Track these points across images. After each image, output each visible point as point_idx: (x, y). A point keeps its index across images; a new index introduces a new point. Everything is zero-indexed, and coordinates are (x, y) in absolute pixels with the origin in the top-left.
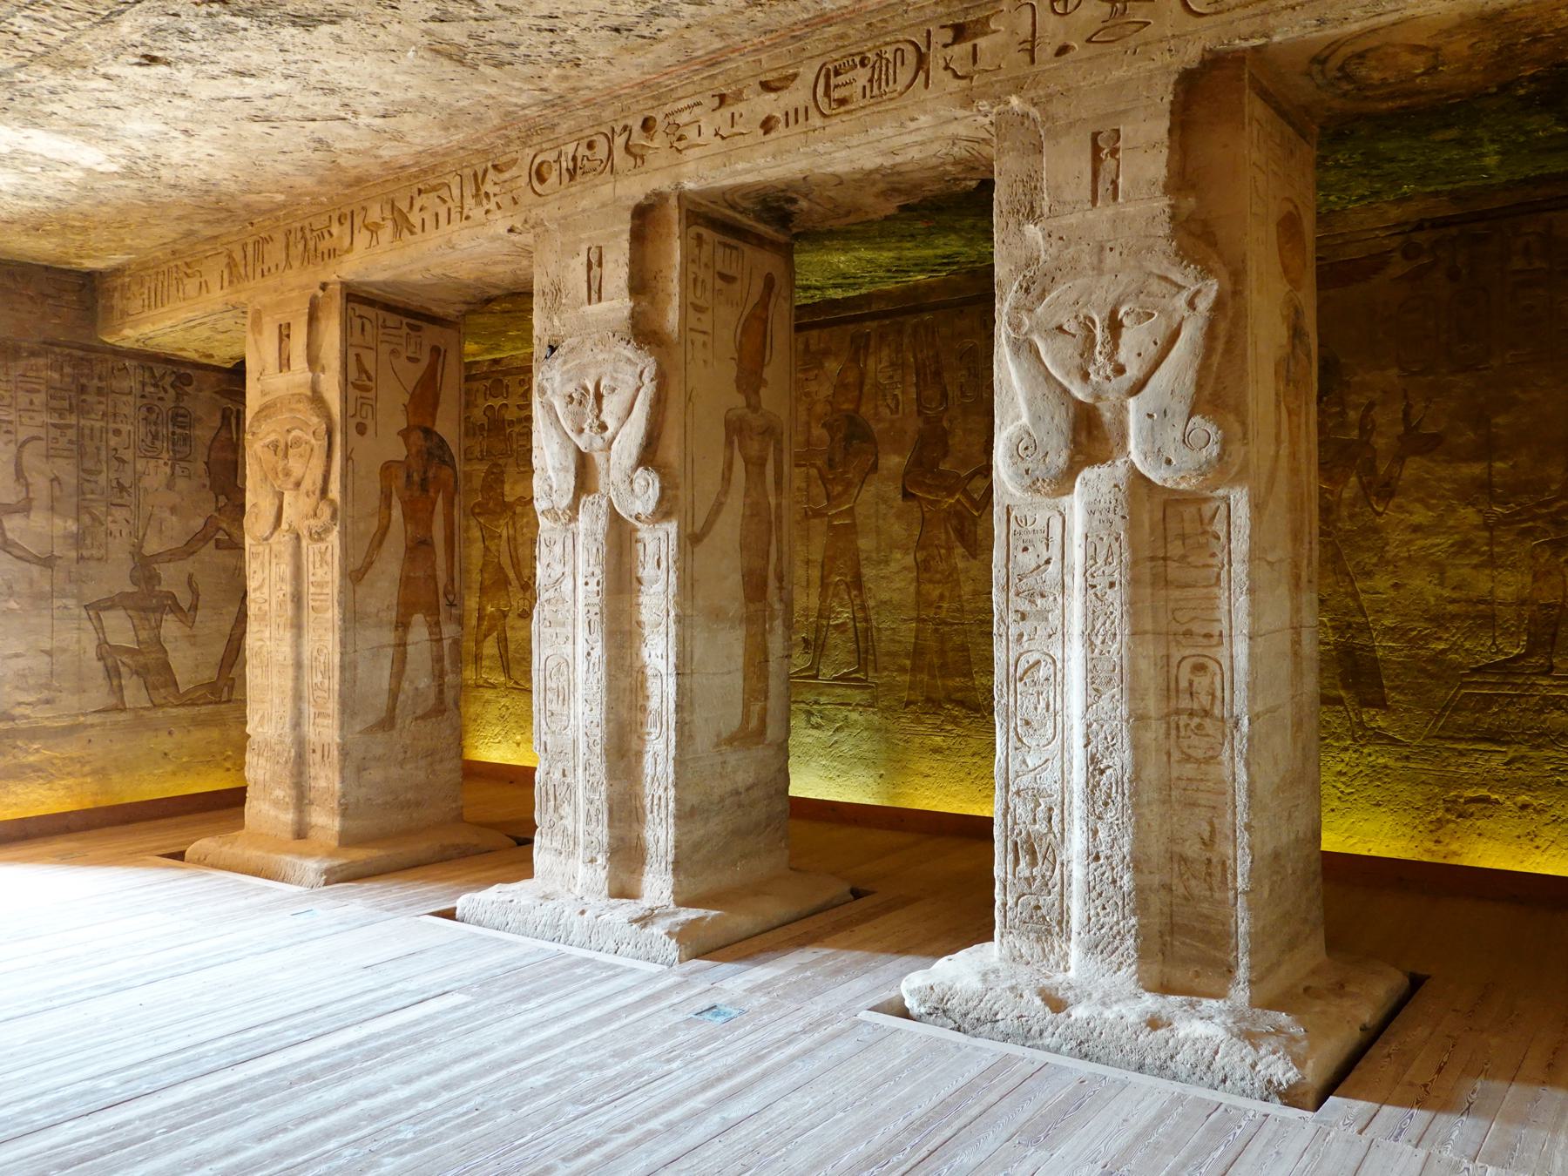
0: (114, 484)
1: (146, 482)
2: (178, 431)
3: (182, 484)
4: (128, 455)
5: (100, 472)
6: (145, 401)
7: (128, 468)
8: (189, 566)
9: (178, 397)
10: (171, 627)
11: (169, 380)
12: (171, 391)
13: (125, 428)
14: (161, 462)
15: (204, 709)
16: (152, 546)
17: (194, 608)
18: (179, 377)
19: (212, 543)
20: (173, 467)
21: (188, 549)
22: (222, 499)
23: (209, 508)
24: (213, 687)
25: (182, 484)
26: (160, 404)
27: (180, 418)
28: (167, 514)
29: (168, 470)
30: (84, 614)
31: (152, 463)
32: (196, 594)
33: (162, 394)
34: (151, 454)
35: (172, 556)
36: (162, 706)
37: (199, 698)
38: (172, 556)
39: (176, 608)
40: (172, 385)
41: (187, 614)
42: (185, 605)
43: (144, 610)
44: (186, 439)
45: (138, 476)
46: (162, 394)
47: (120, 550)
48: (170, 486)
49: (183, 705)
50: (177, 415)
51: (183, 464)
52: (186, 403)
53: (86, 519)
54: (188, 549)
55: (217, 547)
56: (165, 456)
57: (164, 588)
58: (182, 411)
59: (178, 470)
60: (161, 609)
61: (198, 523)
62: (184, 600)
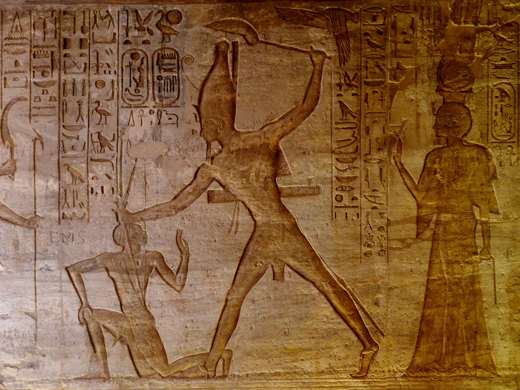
0: (95, 138)
2: (164, 74)
3: (168, 132)
5: (82, 127)
6: (128, 47)
7: (111, 120)
8: (176, 222)
9: (165, 37)
11: (154, 20)
12: (158, 33)
13: (109, 78)
14: (146, 111)
18: (166, 15)
19: (204, 197)
20: (159, 115)
22: (215, 146)
23: (199, 157)
24: (204, 359)
26: (143, 47)
27: (168, 62)
28: (152, 167)
29: (154, 118)
30: (65, 276)
31: (137, 112)
33: (147, 37)
34: (134, 103)
35: (158, 212)
36: (148, 377)
37: (190, 370)
38: (158, 212)
39: (163, 269)
40: (158, 26)
42: (174, 266)
46: (147, 37)
47: (102, 207)
48: (155, 137)
49: (172, 377)
50: (163, 57)
51: (170, 110)
53: (67, 177)
55: (210, 199)
56: (151, 103)
57: (150, 247)
58: (167, 52)
59: (165, 118)
62: (173, 260)
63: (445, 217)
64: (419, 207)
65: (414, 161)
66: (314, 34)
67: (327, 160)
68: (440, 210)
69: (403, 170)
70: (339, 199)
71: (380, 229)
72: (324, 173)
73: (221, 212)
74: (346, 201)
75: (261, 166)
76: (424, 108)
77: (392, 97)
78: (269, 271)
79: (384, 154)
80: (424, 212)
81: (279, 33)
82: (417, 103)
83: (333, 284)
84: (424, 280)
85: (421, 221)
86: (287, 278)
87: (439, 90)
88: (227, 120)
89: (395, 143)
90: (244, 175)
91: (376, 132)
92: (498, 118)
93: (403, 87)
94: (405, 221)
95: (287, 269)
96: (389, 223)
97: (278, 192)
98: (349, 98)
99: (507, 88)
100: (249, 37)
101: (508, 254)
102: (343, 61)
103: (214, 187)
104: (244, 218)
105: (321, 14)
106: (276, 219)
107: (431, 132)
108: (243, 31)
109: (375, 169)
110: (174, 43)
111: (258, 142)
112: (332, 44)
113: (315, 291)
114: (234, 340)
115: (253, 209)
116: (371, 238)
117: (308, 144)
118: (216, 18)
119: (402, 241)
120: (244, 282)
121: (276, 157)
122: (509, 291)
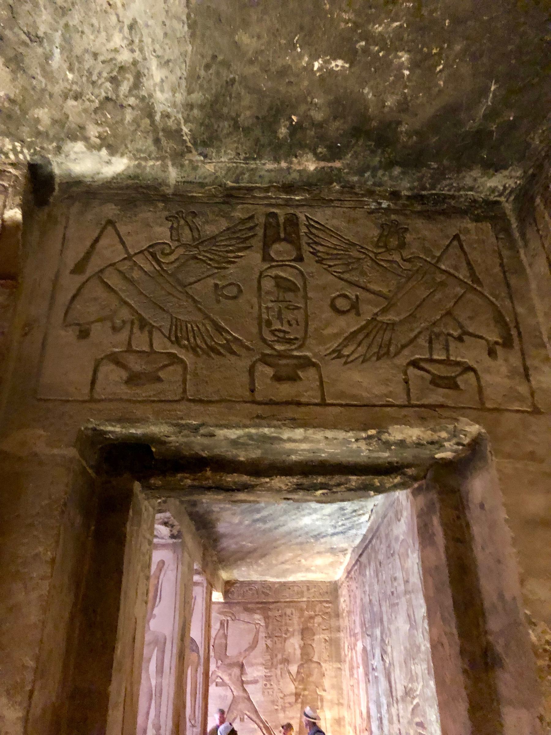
22: (220, 662)
55: (217, 685)
63: (306, 693)
64: (296, 688)
65: (294, 669)
66: (257, 616)
67: (261, 668)
68: (305, 689)
69: (290, 673)
70: (266, 685)
71: (281, 698)
72: (260, 674)
74: (268, 686)
75: (236, 671)
76: (297, 646)
77: (285, 642)
78: (239, 717)
79: (282, 666)
80: (298, 691)
82: (294, 644)
83: (262, 721)
84: (298, 721)
85: (297, 695)
86: (245, 720)
87: (302, 639)
88: (224, 651)
89: (286, 661)
91: (279, 657)
92: (324, 651)
93: (289, 638)
94: (291, 694)
95: (246, 717)
96: (285, 696)
97: (243, 682)
98: (269, 642)
99: (327, 638)
100: (233, 618)
101: (330, 710)
102: (267, 627)
103: (219, 680)
104: (229, 694)
105: (259, 608)
107: (299, 656)
108: (231, 615)
109: (279, 672)
111: (236, 661)
112: (263, 621)
113: (256, 726)
115: (232, 688)
116: (277, 701)
117: (254, 661)
118: (222, 610)
119: (290, 703)
121: (242, 666)
122: (331, 726)
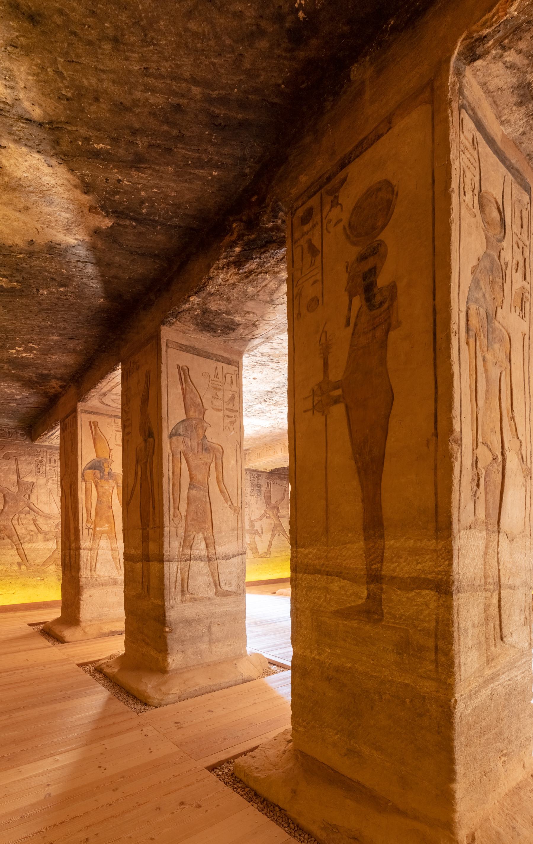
1: (252, 502)
3: (259, 502)
4: (248, 495)
10: (257, 537)
11: (256, 476)
15: (265, 559)
16: (253, 518)
17: (262, 533)
18: (258, 475)
21: (260, 519)
23: (265, 508)
25: (259, 502)
27: (258, 485)
32: (262, 530)
34: (252, 495)
39: (258, 533)
41: (260, 534)
42: (260, 533)
43: (252, 534)
44: (260, 490)
45: (250, 500)
48: (256, 503)
52: (260, 481)
54: (260, 519)
60: (255, 533)
61: (262, 512)
73: (268, 521)
75: (276, 510)
81: (278, 481)
90: (273, 513)
104: (273, 522)
106: (278, 522)
110: (260, 481)
114: (271, 549)
120: (273, 536)
121: (278, 509)
